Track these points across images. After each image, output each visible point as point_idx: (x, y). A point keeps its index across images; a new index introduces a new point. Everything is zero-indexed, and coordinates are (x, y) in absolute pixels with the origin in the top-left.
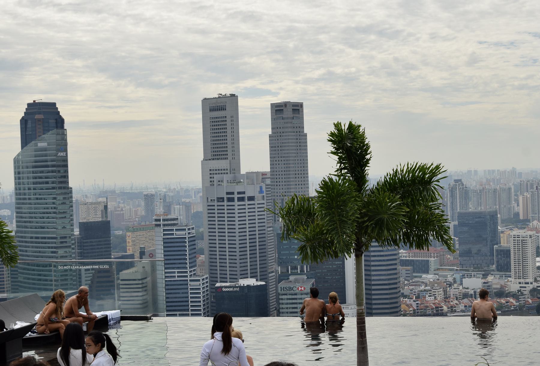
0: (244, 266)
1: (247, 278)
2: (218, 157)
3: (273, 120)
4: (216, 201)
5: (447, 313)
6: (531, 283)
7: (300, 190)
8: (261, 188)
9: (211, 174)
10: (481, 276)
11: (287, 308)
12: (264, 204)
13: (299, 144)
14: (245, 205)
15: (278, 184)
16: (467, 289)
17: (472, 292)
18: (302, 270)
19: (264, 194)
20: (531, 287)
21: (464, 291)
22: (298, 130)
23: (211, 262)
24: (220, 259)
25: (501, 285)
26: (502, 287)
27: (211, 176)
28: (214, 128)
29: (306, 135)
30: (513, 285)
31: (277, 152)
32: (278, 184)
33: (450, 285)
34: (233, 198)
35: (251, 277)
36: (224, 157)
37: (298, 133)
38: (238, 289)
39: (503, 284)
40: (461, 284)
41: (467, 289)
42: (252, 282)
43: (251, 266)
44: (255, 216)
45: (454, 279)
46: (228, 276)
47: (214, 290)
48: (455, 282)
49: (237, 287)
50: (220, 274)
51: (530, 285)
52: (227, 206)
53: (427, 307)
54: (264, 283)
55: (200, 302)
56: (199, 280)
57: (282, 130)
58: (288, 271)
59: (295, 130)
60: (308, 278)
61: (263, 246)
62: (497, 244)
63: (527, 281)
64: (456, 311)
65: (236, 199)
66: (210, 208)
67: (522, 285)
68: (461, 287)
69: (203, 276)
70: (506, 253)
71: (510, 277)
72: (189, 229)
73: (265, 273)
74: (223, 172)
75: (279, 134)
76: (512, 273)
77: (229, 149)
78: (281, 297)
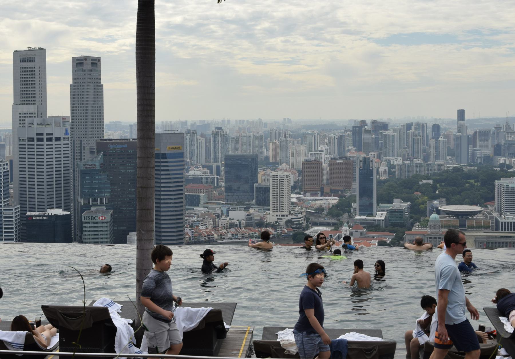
0: (51, 198)
1: (53, 208)
2: (27, 102)
3: (75, 72)
4: (26, 141)
5: (217, 240)
6: (287, 216)
7: (97, 133)
8: (66, 130)
9: (20, 117)
10: (243, 209)
11: (89, 235)
12: (68, 144)
13: (96, 93)
14: (52, 145)
15: (77, 127)
16: (233, 220)
17: (237, 223)
18: (101, 202)
19: (69, 136)
20: (286, 219)
21: (230, 221)
22: (96, 81)
23: (21, 194)
24: (29, 191)
25: (261, 217)
26: (262, 218)
27: (21, 120)
28: (23, 76)
29: (102, 86)
30: (272, 218)
31: (77, 99)
32: (77, 127)
33: (219, 217)
34: (43, 138)
35: (57, 208)
36: (32, 102)
37: (96, 84)
38: (46, 218)
39: (262, 216)
40: (228, 216)
41: (233, 220)
42: (59, 212)
43: (56, 197)
44: (60, 154)
45: (222, 211)
46: (36, 207)
47: (25, 219)
48: (222, 214)
49: (46, 216)
50: (29, 204)
51: (285, 217)
52: (37, 145)
53: (200, 235)
54: (69, 213)
55: (12, 228)
56: (12, 210)
57: (82, 81)
58: (89, 203)
59: (93, 81)
60: (107, 209)
61: (67, 180)
62: (257, 182)
63: (283, 213)
64: (224, 239)
65: (45, 140)
66: (21, 147)
67: (278, 217)
68: (228, 219)
69: (15, 206)
70: (266, 190)
71: (269, 210)
72: (4, 165)
73: (68, 204)
74: (31, 115)
75: (79, 84)
76: (271, 207)
77: (37, 96)
78: (84, 225)
